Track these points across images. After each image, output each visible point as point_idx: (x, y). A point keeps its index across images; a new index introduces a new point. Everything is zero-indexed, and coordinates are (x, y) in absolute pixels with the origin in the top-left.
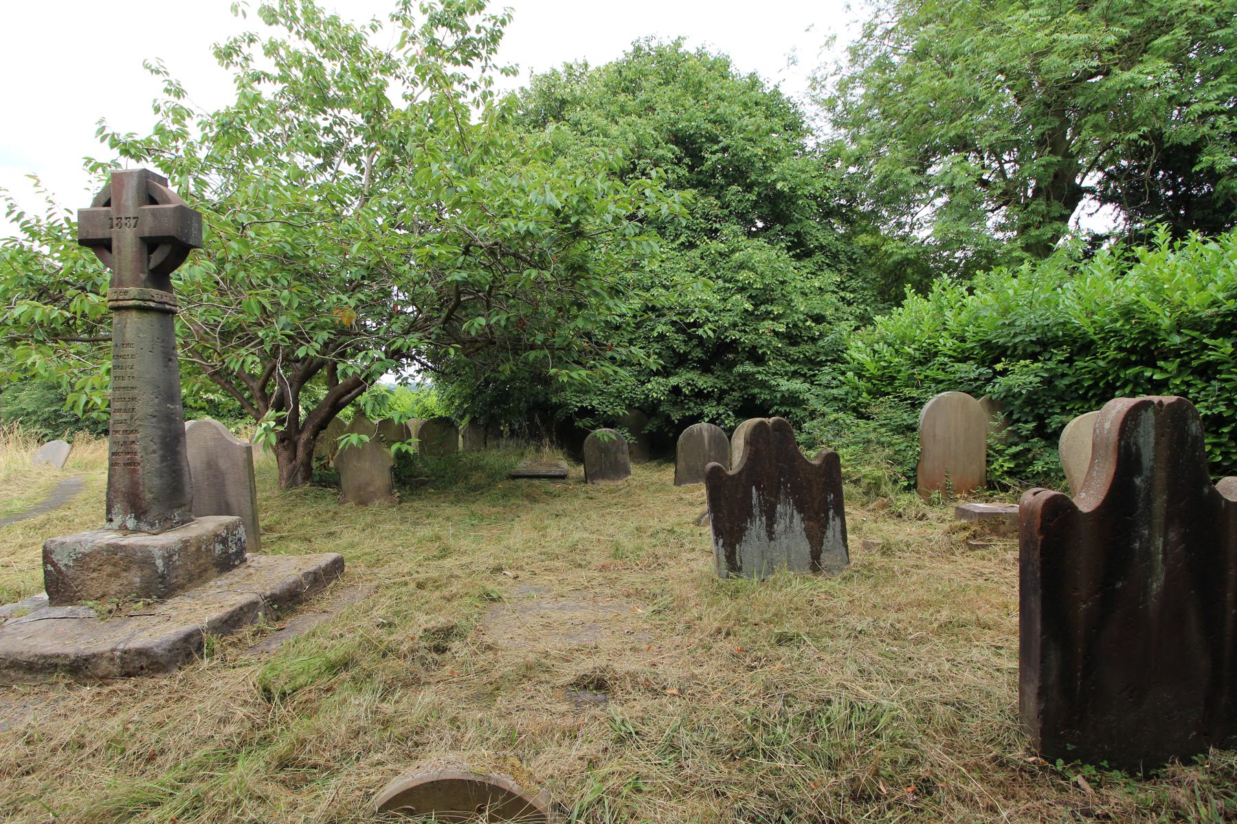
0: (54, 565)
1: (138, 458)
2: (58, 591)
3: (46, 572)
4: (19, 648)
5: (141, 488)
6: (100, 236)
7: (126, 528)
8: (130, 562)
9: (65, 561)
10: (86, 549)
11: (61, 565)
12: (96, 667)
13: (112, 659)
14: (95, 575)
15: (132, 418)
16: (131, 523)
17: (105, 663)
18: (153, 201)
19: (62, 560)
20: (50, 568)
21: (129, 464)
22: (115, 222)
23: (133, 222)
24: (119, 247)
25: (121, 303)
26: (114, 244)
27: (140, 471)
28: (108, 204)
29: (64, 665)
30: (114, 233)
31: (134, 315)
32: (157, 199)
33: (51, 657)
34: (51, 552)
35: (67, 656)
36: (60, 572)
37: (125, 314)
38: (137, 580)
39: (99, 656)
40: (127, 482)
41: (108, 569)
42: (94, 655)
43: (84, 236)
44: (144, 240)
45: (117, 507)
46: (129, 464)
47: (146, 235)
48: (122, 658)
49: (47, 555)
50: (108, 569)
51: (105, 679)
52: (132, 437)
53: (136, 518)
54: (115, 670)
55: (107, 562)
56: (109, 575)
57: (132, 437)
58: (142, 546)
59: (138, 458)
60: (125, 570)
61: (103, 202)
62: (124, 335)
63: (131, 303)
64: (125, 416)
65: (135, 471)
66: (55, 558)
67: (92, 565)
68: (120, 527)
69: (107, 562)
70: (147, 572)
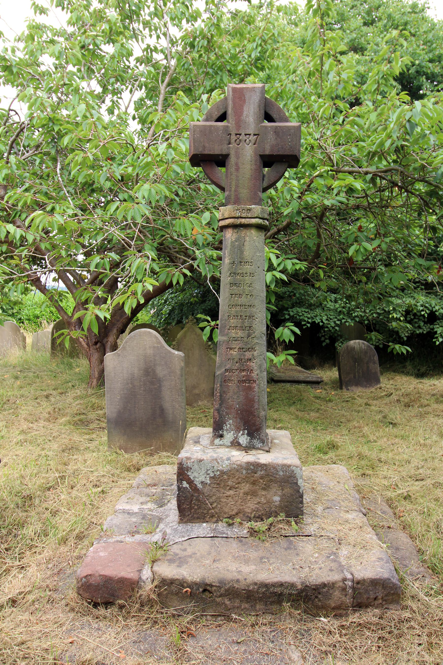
0: (190, 482)
1: (254, 375)
2: (191, 508)
3: (179, 489)
4: (229, 576)
5: (256, 406)
6: (217, 152)
7: (239, 444)
8: (271, 481)
9: (202, 478)
10: (225, 466)
11: (197, 482)
12: (328, 596)
13: (344, 589)
14: (231, 492)
15: (249, 336)
16: (244, 440)
17: (337, 594)
18: (269, 118)
19: (199, 477)
20: (185, 484)
21: (244, 381)
22: (233, 137)
23: (253, 138)
24: (237, 164)
25: (243, 221)
26: (232, 160)
27: (256, 389)
28: (222, 117)
29: (290, 595)
30: (232, 149)
31: (254, 232)
32: (275, 116)
33: (274, 585)
34: (189, 469)
35: (292, 585)
36: (195, 489)
37: (244, 232)
38: (277, 499)
39: (330, 586)
40: (242, 398)
41: (246, 487)
42: (324, 585)
43: (200, 151)
44: (262, 157)
45: (229, 423)
46: (244, 381)
47: (267, 152)
48: (353, 588)
49: (182, 473)
50: (246, 487)
51: (338, 612)
52: (248, 355)
53: (248, 434)
54: (348, 600)
55: (246, 479)
56: (246, 494)
57: (248, 355)
58: (284, 465)
59: (254, 375)
60: (264, 489)
61: (215, 117)
62: (242, 252)
63: (254, 221)
64: (240, 334)
65: (250, 388)
66: (191, 475)
67: (230, 483)
68: (232, 443)
69: (246, 479)
70: (288, 491)
